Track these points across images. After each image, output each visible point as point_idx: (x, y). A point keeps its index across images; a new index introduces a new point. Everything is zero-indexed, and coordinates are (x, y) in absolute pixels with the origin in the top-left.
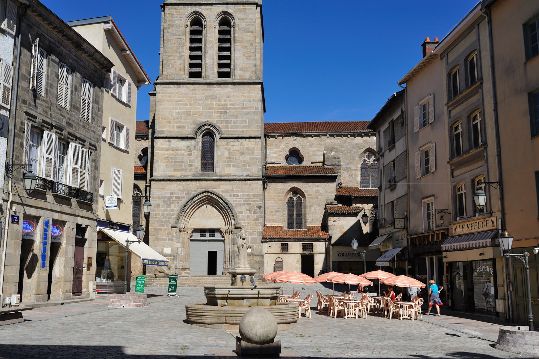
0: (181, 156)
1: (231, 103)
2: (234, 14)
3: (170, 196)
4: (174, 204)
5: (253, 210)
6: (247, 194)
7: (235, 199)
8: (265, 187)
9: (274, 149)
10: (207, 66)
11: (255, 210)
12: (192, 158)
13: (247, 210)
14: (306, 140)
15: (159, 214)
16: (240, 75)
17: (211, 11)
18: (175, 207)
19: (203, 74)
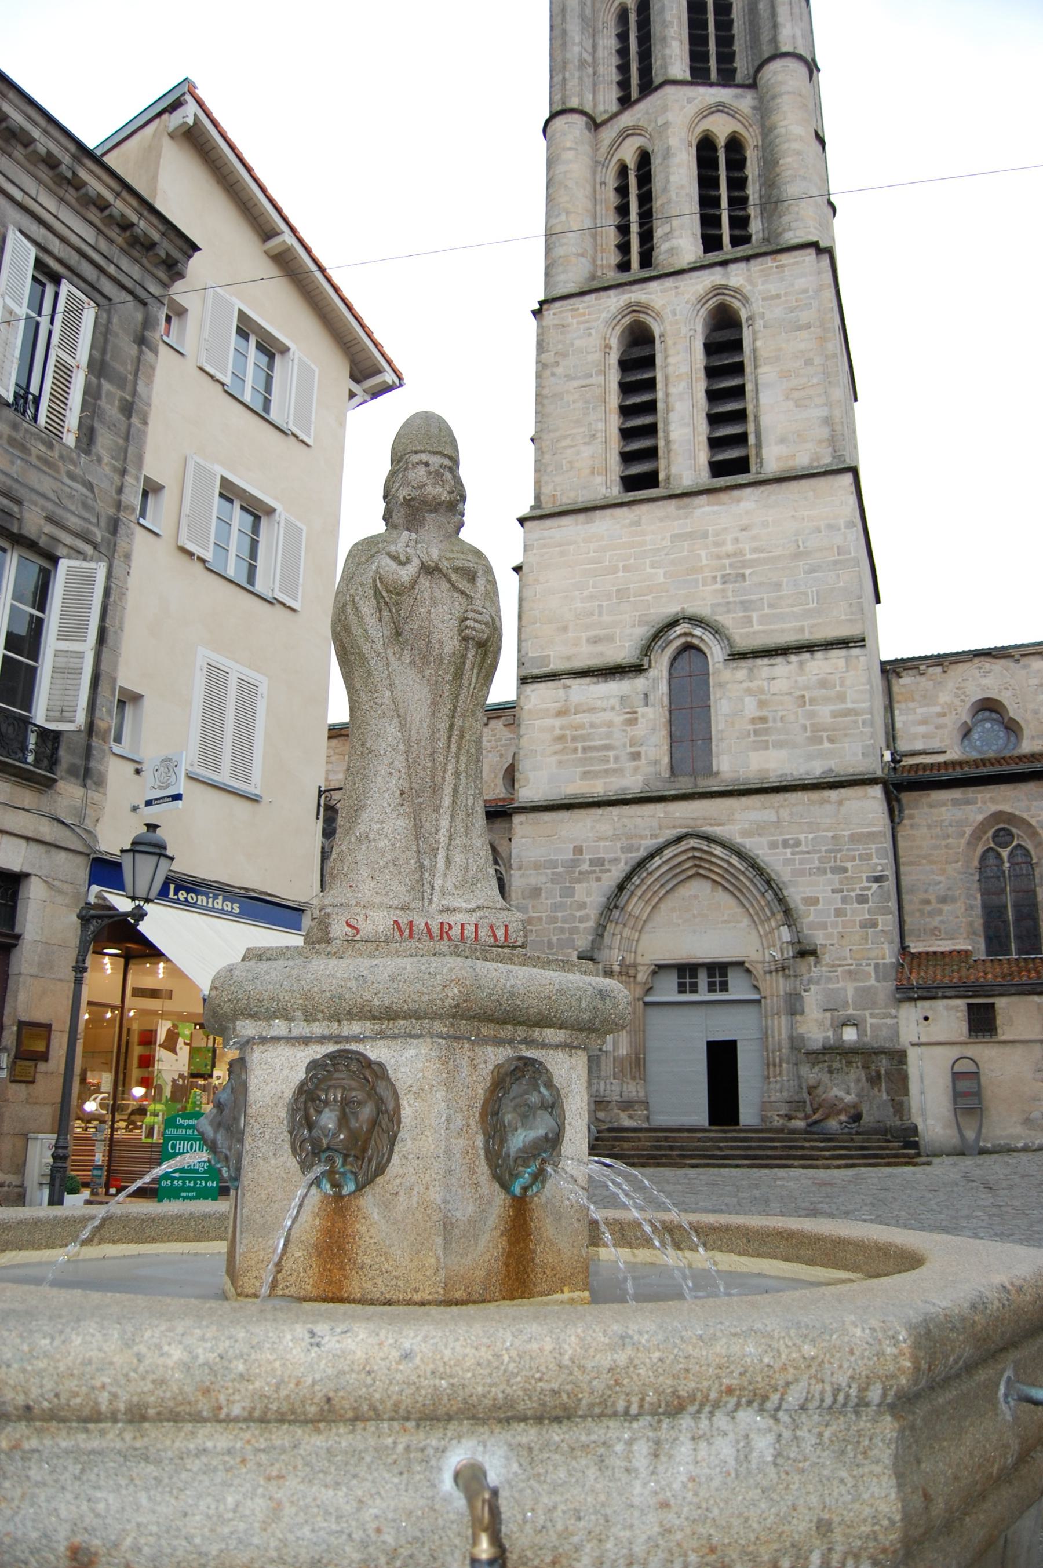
0: (603, 730)
1: (755, 544)
2: (749, 288)
3: (572, 860)
4: (585, 885)
5: (853, 890)
6: (830, 834)
7: (789, 856)
8: (897, 820)
9: (919, 711)
10: (674, 447)
11: (862, 889)
12: (640, 730)
13: (833, 891)
14: (1024, 672)
15: (540, 919)
16: (778, 459)
17: (677, 294)
18: (589, 894)
19: (662, 476)
